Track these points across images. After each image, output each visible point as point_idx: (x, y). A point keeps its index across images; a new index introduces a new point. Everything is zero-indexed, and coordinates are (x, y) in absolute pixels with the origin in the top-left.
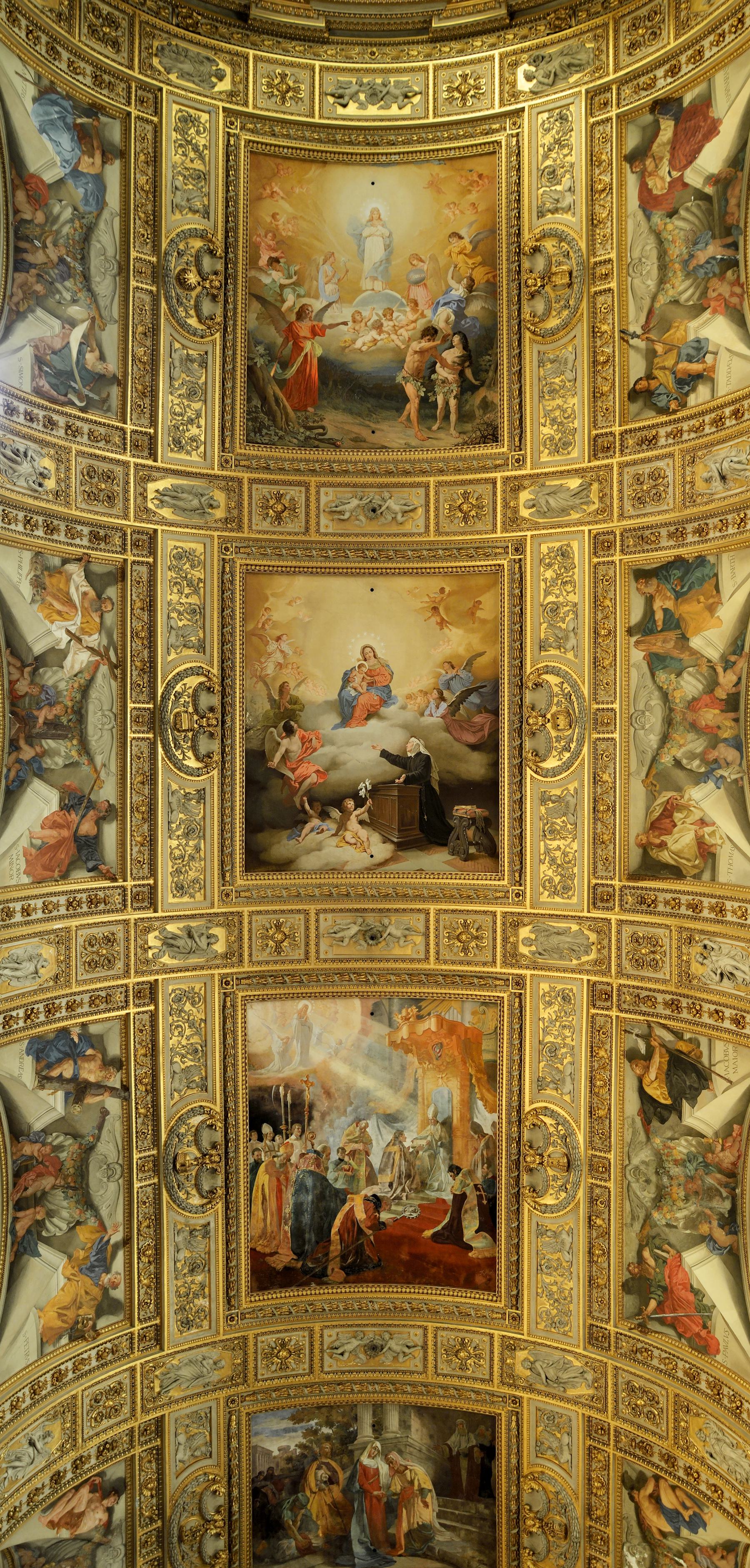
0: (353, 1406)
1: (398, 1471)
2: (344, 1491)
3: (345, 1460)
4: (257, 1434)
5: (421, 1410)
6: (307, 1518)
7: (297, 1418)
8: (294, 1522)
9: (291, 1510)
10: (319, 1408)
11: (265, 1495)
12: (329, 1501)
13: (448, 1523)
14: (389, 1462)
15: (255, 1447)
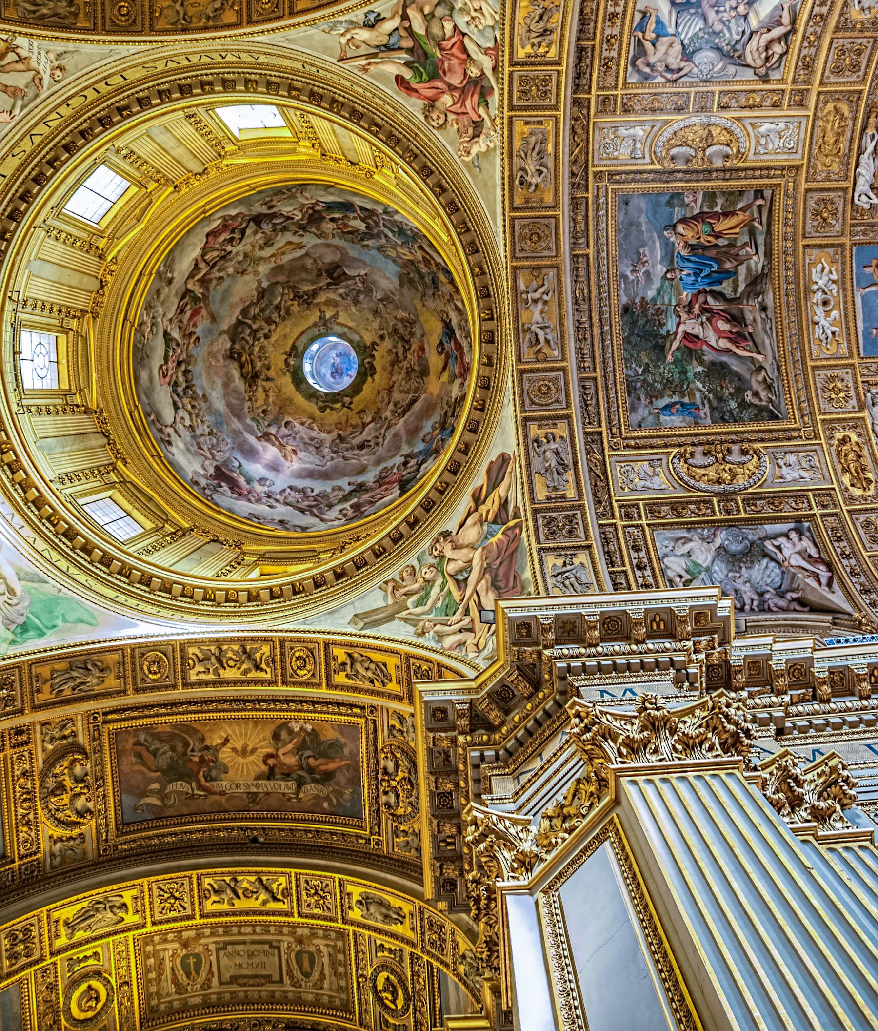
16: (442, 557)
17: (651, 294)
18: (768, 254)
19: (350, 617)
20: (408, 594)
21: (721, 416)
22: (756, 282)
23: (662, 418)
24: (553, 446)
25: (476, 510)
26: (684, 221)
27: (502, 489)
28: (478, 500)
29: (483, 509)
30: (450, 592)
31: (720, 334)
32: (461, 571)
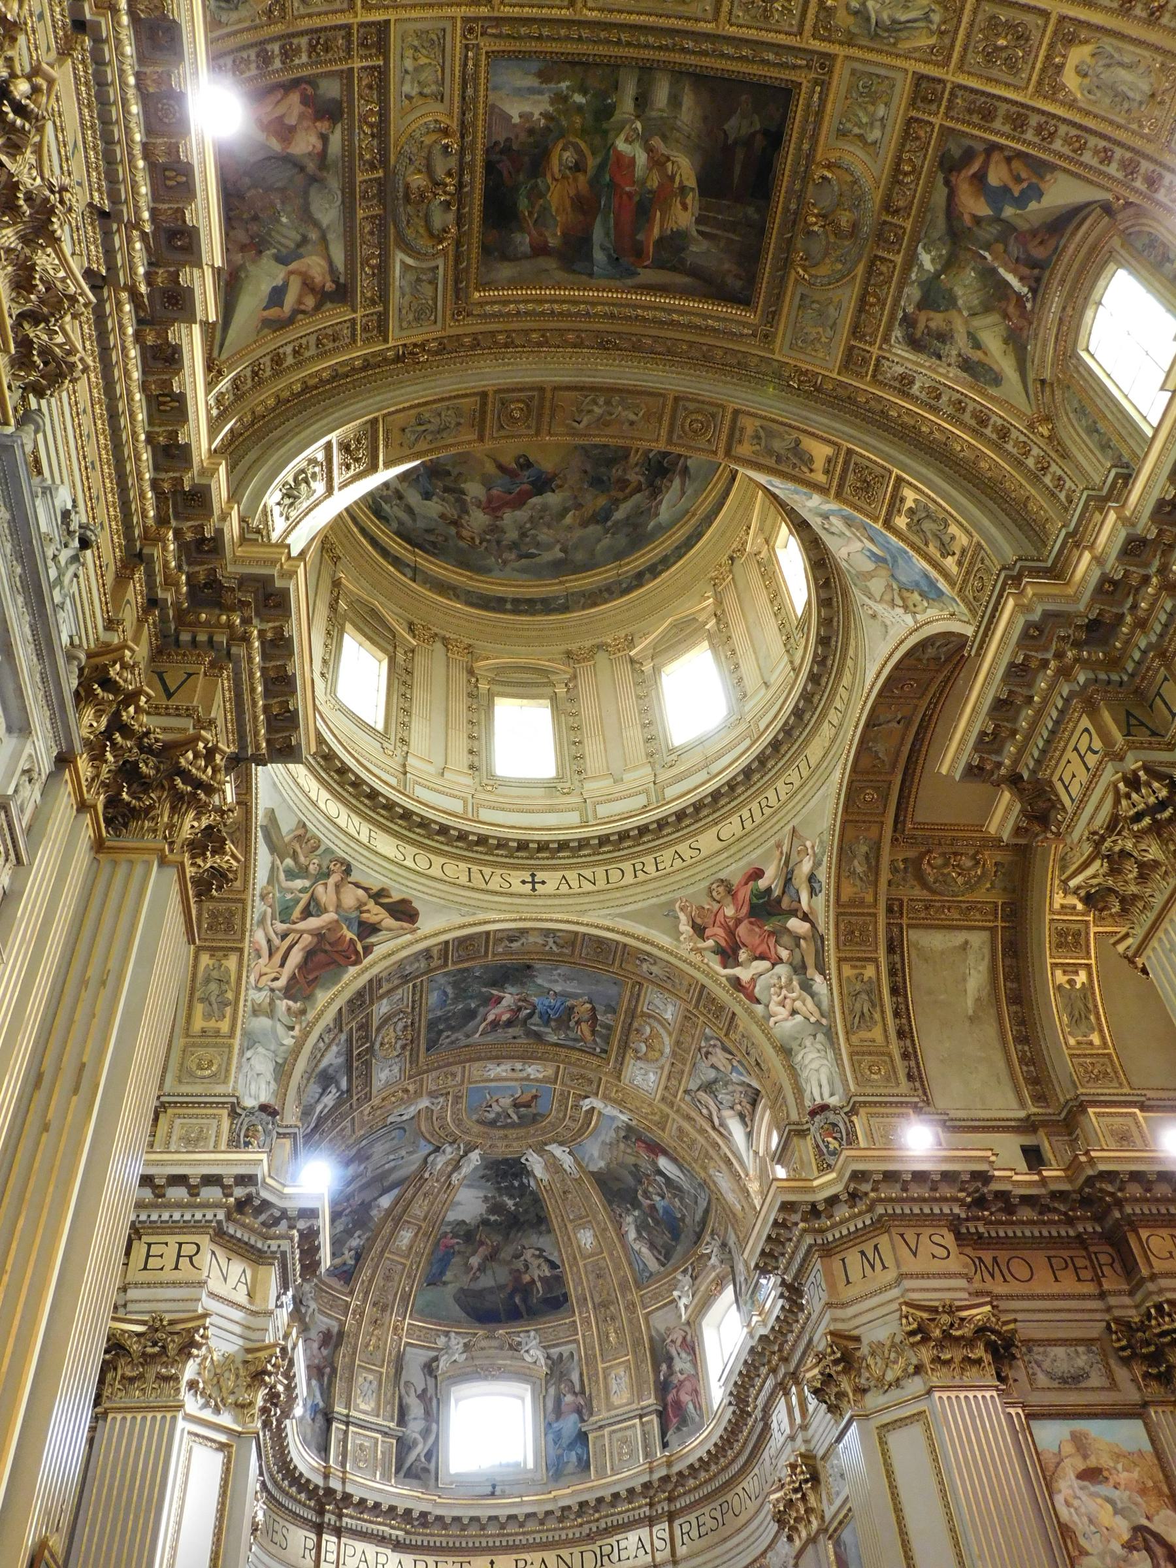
0: (614, 67)
1: (658, 162)
2: (594, 182)
3: (597, 141)
4: (495, 88)
5: (701, 80)
6: (545, 209)
7: (544, 76)
8: (530, 213)
9: (529, 198)
10: (573, 64)
11: (500, 173)
12: (572, 193)
13: (708, 230)
14: (650, 150)
15: (493, 106)
16: (328, 875)
17: (539, 981)
18: (557, 1045)
19: (270, 805)
20: (295, 856)
21: (432, 1024)
22: (538, 1037)
23: (436, 994)
24: (423, 964)
25: (370, 896)
26: (593, 1009)
27: (389, 922)
28: (378, 895)
29: (371, 905)
30: (298, 901)
31: (499, 1015)
32: (318, 904)
